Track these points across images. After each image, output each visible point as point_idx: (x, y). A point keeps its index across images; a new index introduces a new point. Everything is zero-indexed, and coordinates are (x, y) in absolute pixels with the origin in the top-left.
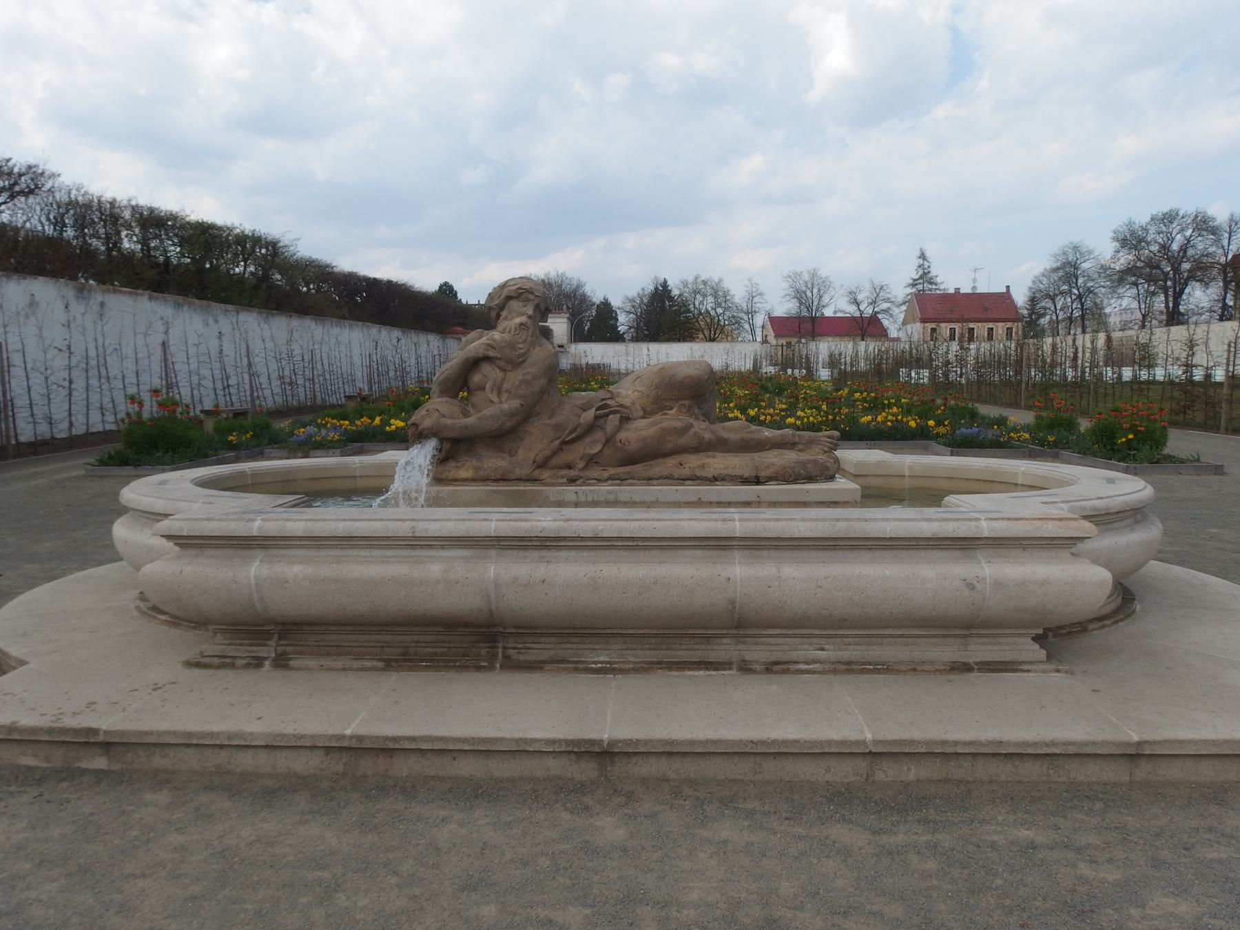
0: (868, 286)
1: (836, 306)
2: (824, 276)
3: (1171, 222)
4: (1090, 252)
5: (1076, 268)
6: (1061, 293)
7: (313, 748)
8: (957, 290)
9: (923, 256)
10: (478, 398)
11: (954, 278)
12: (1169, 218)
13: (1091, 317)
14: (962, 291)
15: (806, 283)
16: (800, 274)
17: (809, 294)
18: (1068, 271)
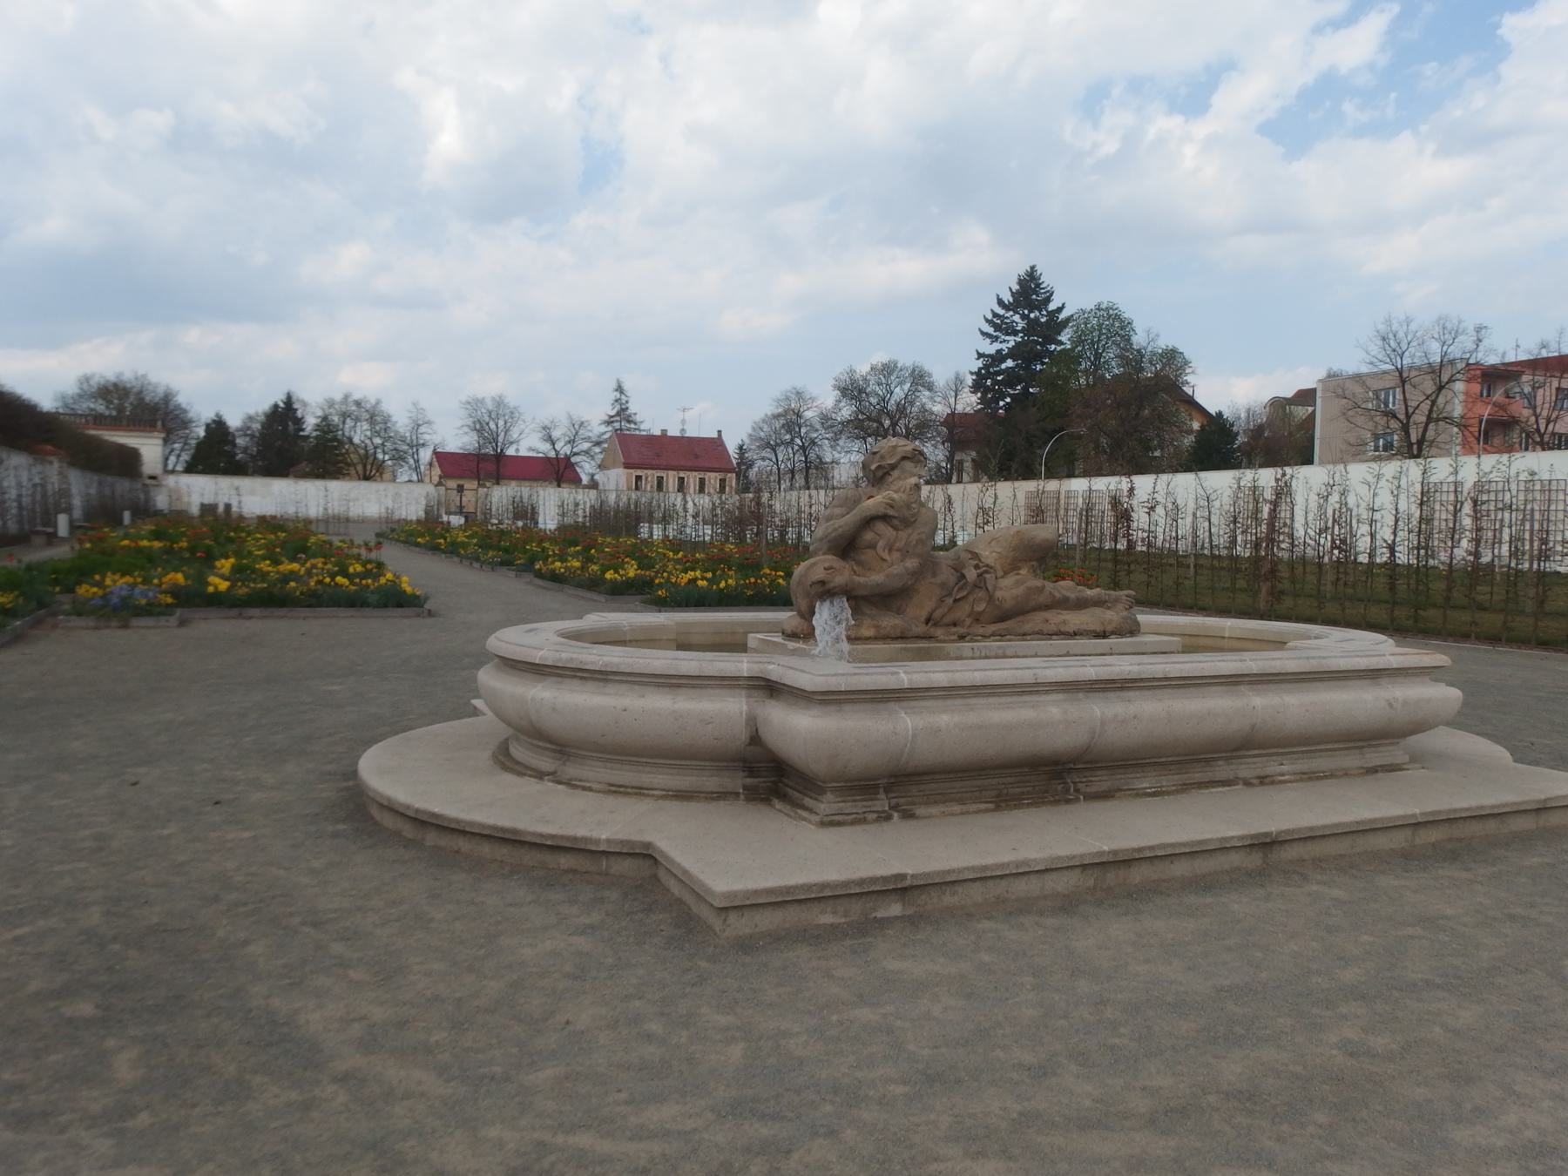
0: (566, 422)
1: (527, 443)
2: (512, 405)
3: (890, 374)
4: (813, 399)
5: (799, 415)
9: (620, 389)
10: (868, 556)
11: (654, 419)
12: (888, 369)
13: (813, 471)
17: (492, 426)
18: (790, 421)
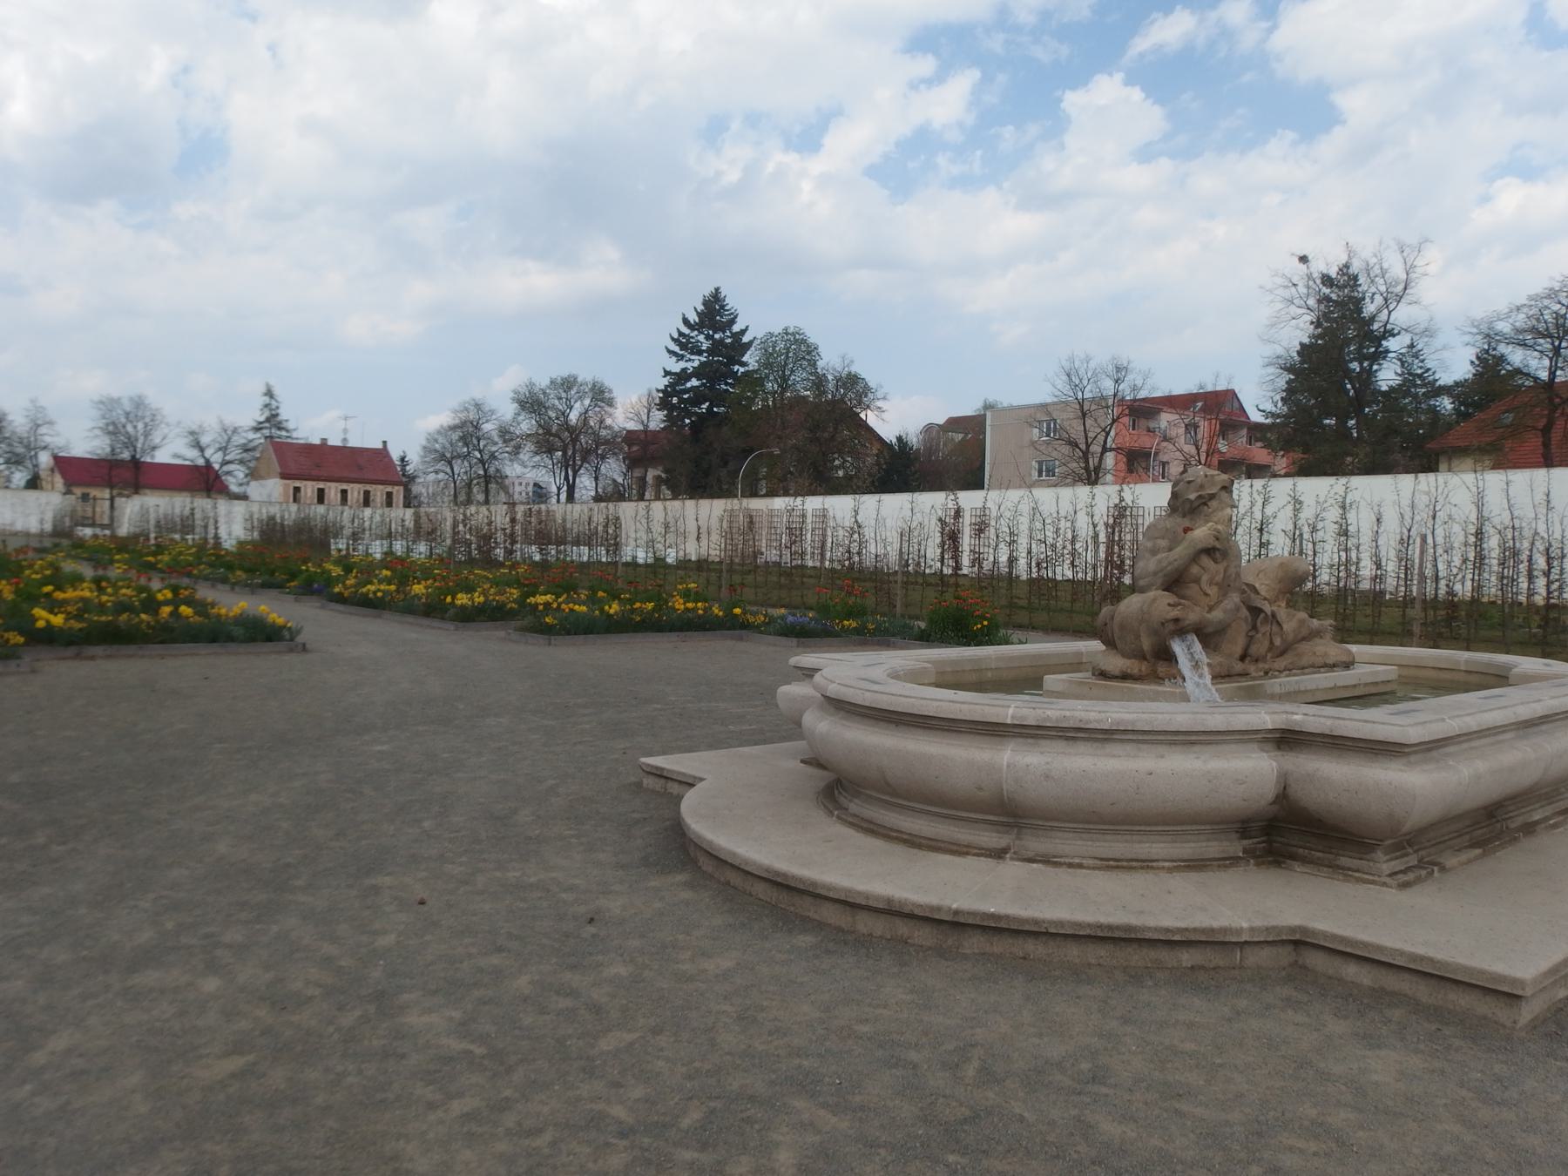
0: (217, 427)
1: (170, 450)
2: (154, 406)
3: (570, 388)
4: (493, 412)
5: (477, 427)
6: (459, 456)
7: (1283, 942)
8: (324, 440)
9: (269, 393)
10: (1193, 590)
11: (313, 424)
12: (568, 384)
13: (491, 481)
14: (330, 443)
15: (127, 414)
16: (118, 401)
17: (130, 428)
18: (468, 432)
